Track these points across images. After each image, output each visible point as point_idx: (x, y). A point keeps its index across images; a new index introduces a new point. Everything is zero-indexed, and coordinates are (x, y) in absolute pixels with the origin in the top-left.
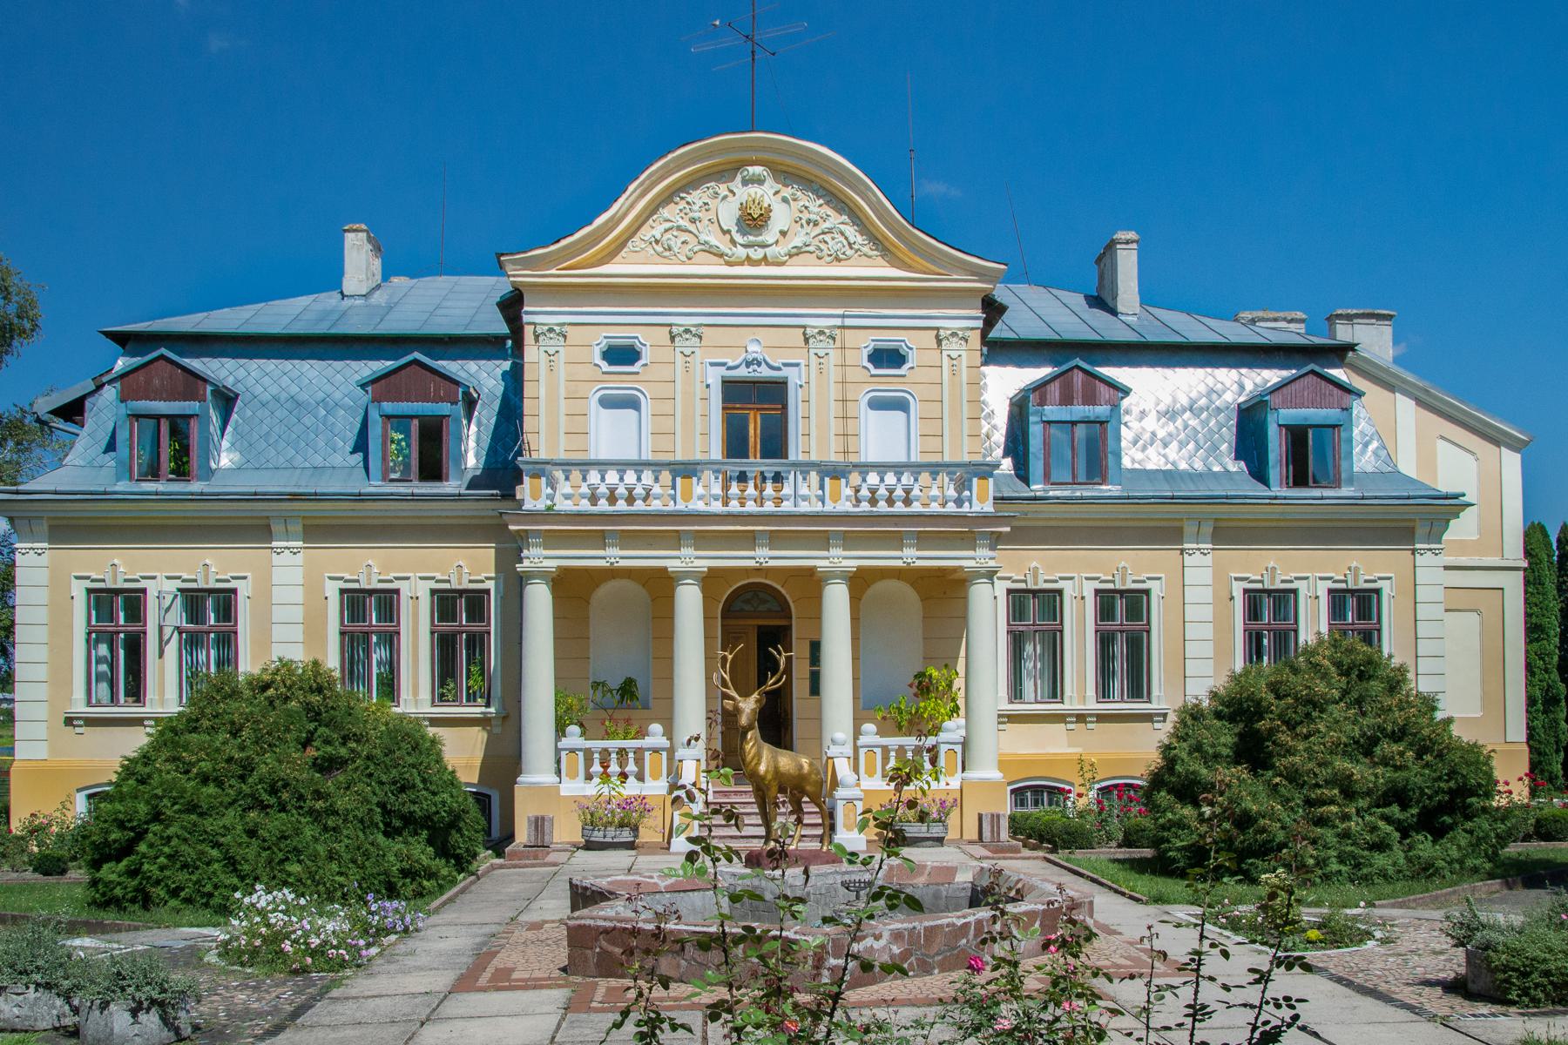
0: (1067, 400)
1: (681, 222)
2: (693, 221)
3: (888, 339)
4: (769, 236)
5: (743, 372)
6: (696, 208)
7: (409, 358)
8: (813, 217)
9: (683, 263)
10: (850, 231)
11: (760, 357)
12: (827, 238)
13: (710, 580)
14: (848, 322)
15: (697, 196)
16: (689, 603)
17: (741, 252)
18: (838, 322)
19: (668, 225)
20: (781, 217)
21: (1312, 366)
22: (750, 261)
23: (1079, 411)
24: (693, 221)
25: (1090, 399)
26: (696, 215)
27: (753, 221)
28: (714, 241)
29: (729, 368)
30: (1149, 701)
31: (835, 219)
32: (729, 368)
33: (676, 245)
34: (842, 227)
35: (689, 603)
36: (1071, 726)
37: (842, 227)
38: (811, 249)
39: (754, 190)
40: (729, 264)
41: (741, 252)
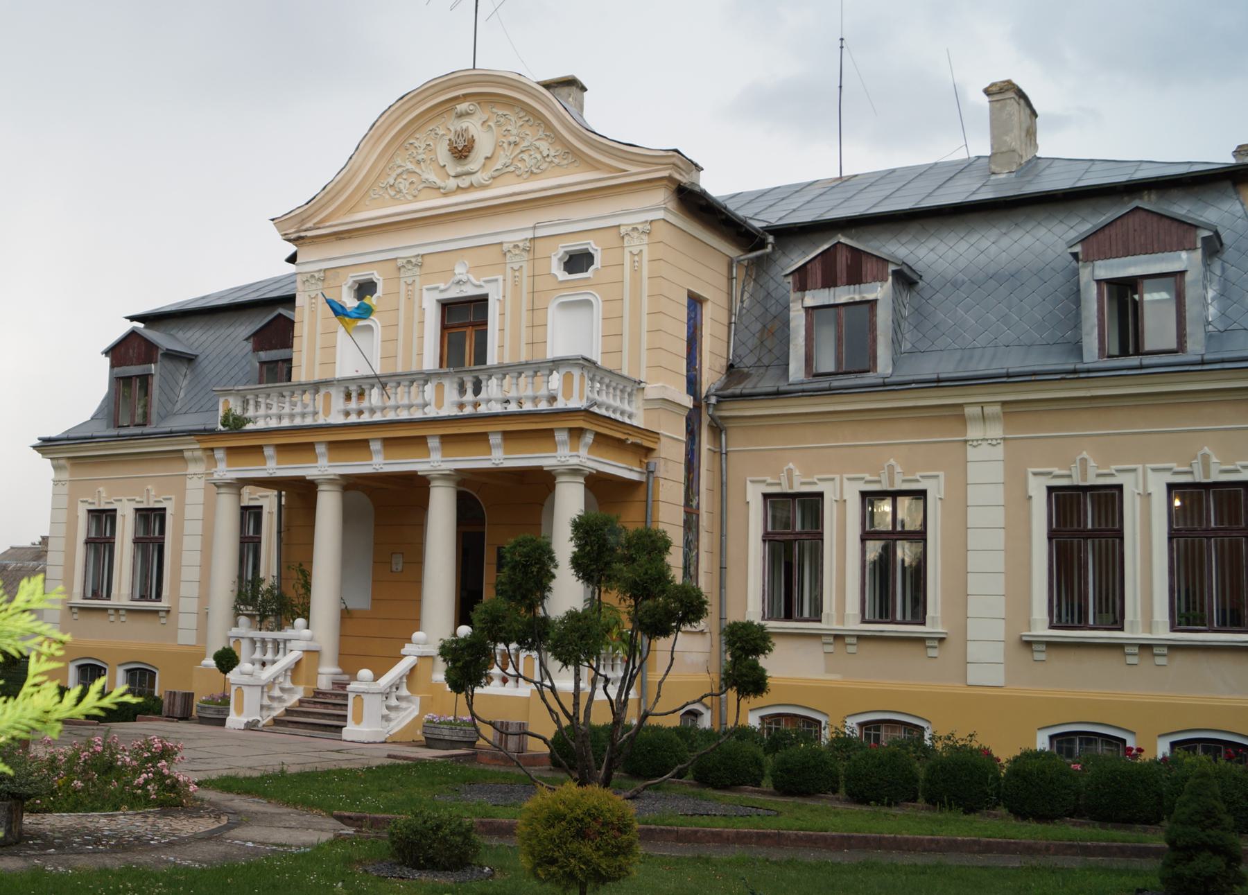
0: (829, 282)
1: (410, 166)
2: (418, 162)
3: (576, 245)
4: (474, 163)
5: (454, 293)
6: (421, 151)
7: (275, 313)
8: (512, 139)
9: (410, 202)
10: (544, 146)
11: (464, 278)
12: (525, 156)
13: (349, 484)
14: (540, 233)
15: (420, 140)
16: (328, 506)
17: (452, 183)
18: (529, 235)
19: (400, 170)
20: (484, 143)
21: (1137, 203)
22: (459, 189)
23: (843, 294)
24: (418, 162)
25: (855, 278)
26: (420, 157)
27: (462, 152)
28: (433, 177)
29: (442, 291)
30: (924, 624)
31: (532, 136)
32: (442, 291)
33: (403, 185)
34: (537, 143)
35: (328, 506)
36: (830, 648)
37: (537, 143)
38: (512, 169)
39: (465, 123)
40: (445, 195)
41: (452, 183)
